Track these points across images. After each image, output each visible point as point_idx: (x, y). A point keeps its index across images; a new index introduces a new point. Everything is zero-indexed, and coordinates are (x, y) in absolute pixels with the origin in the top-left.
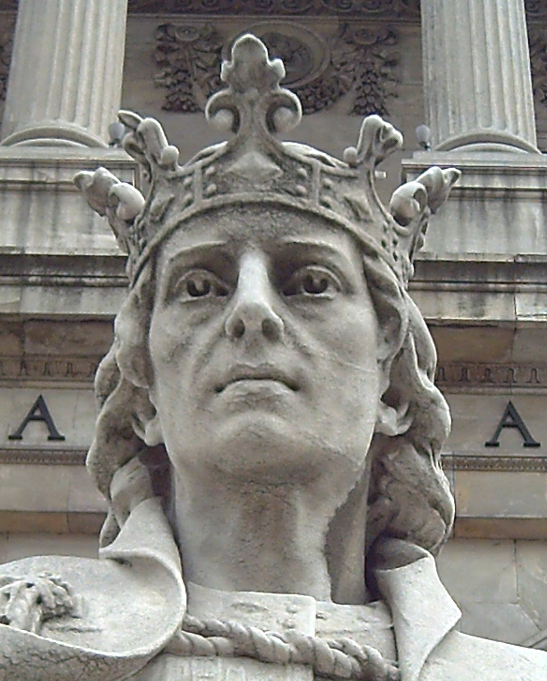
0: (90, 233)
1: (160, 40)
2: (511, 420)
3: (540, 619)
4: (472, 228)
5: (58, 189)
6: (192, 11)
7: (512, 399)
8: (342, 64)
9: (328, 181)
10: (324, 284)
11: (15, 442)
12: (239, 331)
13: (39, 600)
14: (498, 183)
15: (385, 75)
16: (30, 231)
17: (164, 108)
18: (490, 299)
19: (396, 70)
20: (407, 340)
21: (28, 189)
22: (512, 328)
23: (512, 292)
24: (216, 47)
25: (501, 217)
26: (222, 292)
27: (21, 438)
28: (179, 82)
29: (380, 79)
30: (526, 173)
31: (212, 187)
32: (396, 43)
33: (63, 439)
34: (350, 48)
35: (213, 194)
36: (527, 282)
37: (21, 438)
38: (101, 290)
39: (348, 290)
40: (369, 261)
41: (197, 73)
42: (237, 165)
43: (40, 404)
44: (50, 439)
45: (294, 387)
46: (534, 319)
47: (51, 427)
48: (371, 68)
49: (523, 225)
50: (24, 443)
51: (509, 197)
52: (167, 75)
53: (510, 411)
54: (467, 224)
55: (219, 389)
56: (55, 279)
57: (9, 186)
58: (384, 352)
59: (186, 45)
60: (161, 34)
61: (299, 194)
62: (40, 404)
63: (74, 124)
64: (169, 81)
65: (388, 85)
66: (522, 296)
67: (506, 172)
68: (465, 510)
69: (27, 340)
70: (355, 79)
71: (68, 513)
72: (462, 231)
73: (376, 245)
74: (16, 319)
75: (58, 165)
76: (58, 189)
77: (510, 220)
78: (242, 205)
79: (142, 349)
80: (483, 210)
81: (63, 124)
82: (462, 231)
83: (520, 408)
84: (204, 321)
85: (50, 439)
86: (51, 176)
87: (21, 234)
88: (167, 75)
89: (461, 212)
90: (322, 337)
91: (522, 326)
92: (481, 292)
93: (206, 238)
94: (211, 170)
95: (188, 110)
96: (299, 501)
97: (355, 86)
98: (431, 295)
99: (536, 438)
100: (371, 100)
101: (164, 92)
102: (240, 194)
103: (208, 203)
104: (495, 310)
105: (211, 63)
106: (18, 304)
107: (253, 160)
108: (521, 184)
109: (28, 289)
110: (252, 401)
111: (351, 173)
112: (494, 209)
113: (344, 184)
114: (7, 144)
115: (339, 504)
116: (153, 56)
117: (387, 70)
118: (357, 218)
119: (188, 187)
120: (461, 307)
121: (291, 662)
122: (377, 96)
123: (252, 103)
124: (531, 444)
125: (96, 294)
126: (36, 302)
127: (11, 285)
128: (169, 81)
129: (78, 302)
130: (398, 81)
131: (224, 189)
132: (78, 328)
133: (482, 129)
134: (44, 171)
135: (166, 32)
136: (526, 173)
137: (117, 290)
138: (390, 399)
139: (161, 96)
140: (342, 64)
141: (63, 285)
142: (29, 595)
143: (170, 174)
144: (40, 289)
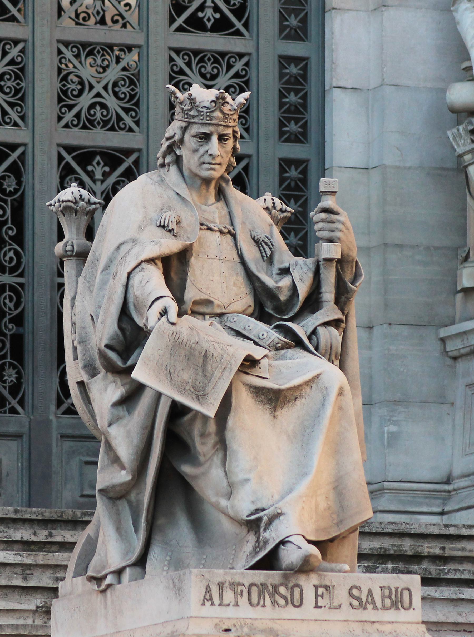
9: (231, 116)
26: (206, 139)
45: (220, 164)
78: (214, 124)
93: (206, 130)
94: (208, 114)
102: (214, 122)
107: (217, 114)
123: (220, 102)
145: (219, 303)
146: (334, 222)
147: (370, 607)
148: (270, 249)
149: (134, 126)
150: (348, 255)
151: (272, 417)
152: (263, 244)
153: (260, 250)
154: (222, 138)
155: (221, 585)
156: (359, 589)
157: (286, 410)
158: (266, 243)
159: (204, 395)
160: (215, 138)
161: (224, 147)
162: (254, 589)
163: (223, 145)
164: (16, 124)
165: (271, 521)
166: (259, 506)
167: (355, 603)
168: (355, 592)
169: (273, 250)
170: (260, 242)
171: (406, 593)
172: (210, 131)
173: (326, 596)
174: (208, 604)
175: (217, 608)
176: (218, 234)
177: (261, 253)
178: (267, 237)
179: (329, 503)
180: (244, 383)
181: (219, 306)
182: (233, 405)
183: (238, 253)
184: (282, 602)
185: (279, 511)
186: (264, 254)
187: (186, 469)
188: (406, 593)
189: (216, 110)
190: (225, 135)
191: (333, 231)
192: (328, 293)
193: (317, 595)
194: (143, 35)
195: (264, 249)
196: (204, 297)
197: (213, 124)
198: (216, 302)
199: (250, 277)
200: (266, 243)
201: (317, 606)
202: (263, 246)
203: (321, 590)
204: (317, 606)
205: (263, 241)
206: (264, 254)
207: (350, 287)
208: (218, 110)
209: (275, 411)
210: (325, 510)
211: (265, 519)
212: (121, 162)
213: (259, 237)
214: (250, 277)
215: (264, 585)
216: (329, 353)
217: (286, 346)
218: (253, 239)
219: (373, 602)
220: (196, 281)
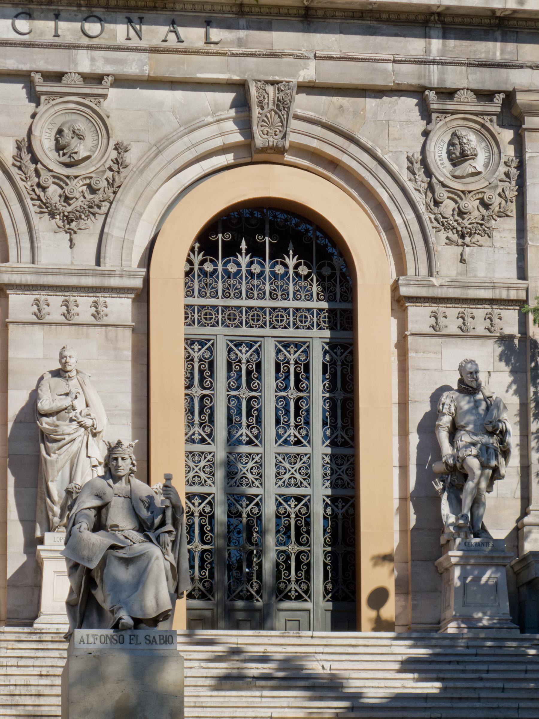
68: (152, 72)
124: (180, 41)
147: (154, 643)
149: (308, 486)
155: (88, 635)
156: (149, 636)
162: (103, 637)
164: (258, 487)
167: (148, 642)
168: (147, 637)
171: (170, 638)
173: (135, 639)
174: (82, 643)
175: (86, 645)
184: (115, 642)
187: (93, 592)
188: (170, 638)
192: (169, 520)
193: (130, 639)
194: (311, 449)
201: (130, 643)
203: (132, 637)
204: (130, 643)
212: (302, 500)
215: (107, 635)
217: (143, 542)
219: (156, 641)
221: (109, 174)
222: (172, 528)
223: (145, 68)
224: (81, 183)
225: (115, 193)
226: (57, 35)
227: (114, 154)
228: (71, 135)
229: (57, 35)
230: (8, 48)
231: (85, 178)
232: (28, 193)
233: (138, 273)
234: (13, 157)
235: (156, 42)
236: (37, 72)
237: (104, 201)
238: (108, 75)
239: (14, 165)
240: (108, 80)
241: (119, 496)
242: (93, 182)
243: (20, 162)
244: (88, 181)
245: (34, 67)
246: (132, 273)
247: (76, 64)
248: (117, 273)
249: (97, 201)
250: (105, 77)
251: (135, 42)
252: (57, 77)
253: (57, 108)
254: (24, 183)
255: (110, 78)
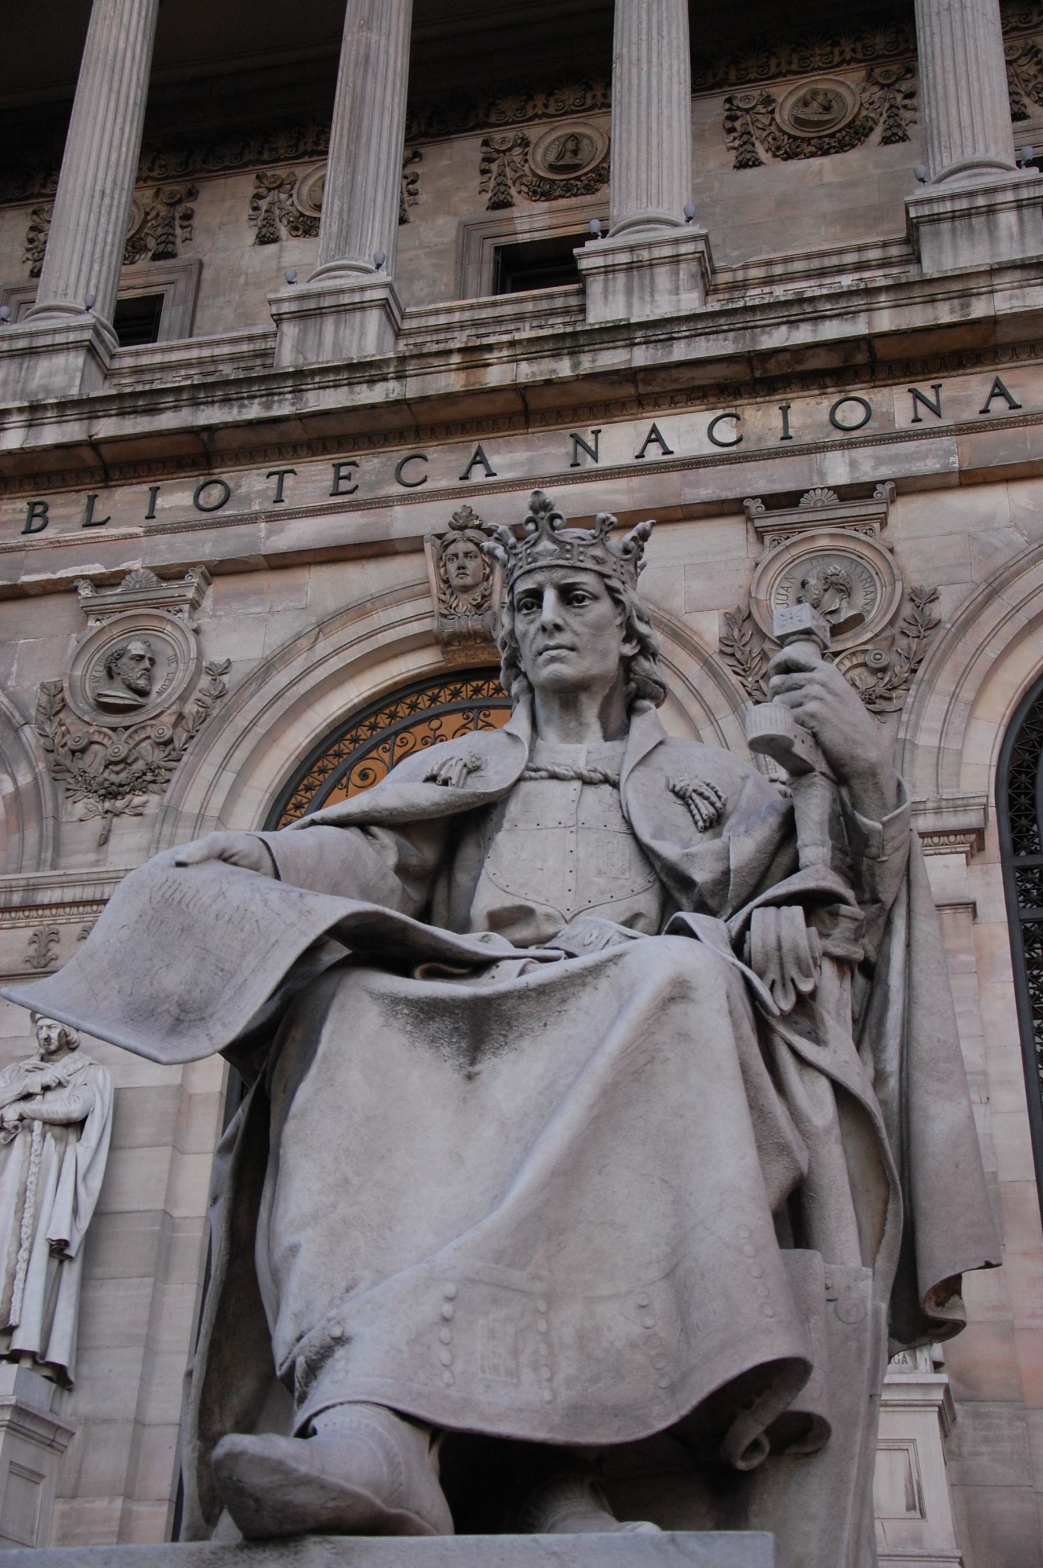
0: (678, 294)
1: (727, 110)
2: (999, 391)
3: (1029, 536)
4: (962, 242)
5: (652, 264)
6: (750, 81)
7: (999, 374)
8: (870, 104)
9: (581, 549)
10: (584, 598)
11: (640, 460)
12: (544, 629)
13: (465, 765)
14: (981, 201)
15: (905, 107)
16: (636, 300)
17: (735, 167)
18: (974, 301)
19: (914, 101)
20: (631, 612)
21: (630, 267)
22: (993, 321)
23: (992, 292)
24: (771, 108)
25: (985, 230)
27: (643, 456)
28: (745, 143)
29: (902, 111)
30: (1003, 189)
31: (530, 560)
32: (913, 77)
33: (672, 452)
34: (875, 89)
35: (530, 563)
36: (1004, 280)
37: (643, 456)
38: (686, 340)
39: (595, 598)
40: (607, 581)
41: (758, 133)
42: (540, 548)
43: (654, 430)
44: (663, 454)
45: (572, 649)
46: (1009, 311)
47: (663, 445)
48: (893, 102)
49: (1003, 232)
50: (645, 460)
51: (991, 210)
52: (735, 139)
53: (997, 384)
54: (958, 240)
55: (540, 654)
56: (653, 338)
57: (617, 267)
58: (619, 620)
59: (747, 111)
60: (728, 106)
61: (568, 559)
62: (654, 430)
63: (660, 210)
64: (737, 143)
65: (908, 115)
66: (1000, 293)
67: (988, 191)
68: (966, 464)
69: (640, 384)
70: (881, 115)
71: (681, 506)
72: (955, 246)
73: (609, 572)
74: (630, 372)
75: (650, 246)
76: (652, 264)
77: (992, 230)
79: (512, 632)
80: (970, 226)
81: (652, 212)
82: (955, 246)
83: (1005, 379)
84: (532, 621)
85: (663, 454)
86: (645, 255)
87: (629, 306)
88: (735, 139)
89: (953, 230)
90: (584, 624)
91: (1001, 318)
92: (966, 295)
94: (529, 551)
95: (754, 165)
96: (584, 698)
97: (882, 120)
98: (929, 306)
99: (1017, 401)
100: (895, 130)
101: (734, 153)
103: (527, 567)
104: (979, 309)
105: (767, 123)
106: (630, 360)
107: (546, 545)
108: (1000, 198)
109: (636, 348)
110: (553, 660)
111: (594, 541)
112: (978, 222)
113: (590, 548)
114: (613, 236)
115: (605, 694)
116: (724, 126)
117: (907, 102)
118: (598, 563)
119: (520, 559)
120: (952, 311)
121: (572, 778)
122: (899, 126)
123: (542, 519)
124: (1014, 406)
125: (683, 343)
126: (641, 357)
127: (622, 347)
128: (737, 143)
129: (671, 352)
130: (915, 109)
131: (535, 560)
132: (673, 371)
133: (969, 157)
134: (639, 252)
135: (732, 104)
136: (1003, 189)
137: (697, 339)
138: (627, 640)
139: (732, 157)
140: (870, 104)
141: (660, 341)
142: (461, 764)
143: (514, 551)
144: (644, 346)
145: (550, 910)
146: (801, 687)
148: (712, 804)
150: (852, 757)
151: (457, 1078)
152: (694, 795)
153: (691, 812)
154: (569, 596)
157: (512, 1056)
158: (701, 794)
159: (202, 1019)
160: (550, 596)
161: (580, 615)
163: (578, 610)
165: (313, 1369)
166: (304, 1326)
169: (718, 805)
170: (688, 794)
172: (536, 583)
176: (577, 784)
177: (693, 816)
178: (708, 785)
179: (649, 1322)
180: (371, 993)
181: (549, 917)
182: (322, 1049)
183: (624, 817)
185: (337, 1332)
186: (698, 817)
189: (539, 537)
190: (572, 587)
191: (800, 705)
195: (696, 806)
196: (508, 902)
197: (541, 568)
198: (540, 910)
199: (646, 854)
200: (701, 794)
202: (693, 801)
205: (694, 791)
206: (698, 817)
207: (865, 825)
208: (544, 537)
209: (473, 1062)
210: (633, 1346)
211: (301, 1361)
213: (682, 784)
214: (646, 854)
216: (775, 960)
218: (673, 791)
220: (498, 874)
221: (903, 642)
222: (834, 883)
223: (952, 459)
224: (848, 664)
225: (914, 671)
226: (786, 437)
227: (908, 610)
228: (821, 586)
229: (786, 437)
230: (701, 470)
231: (854, 654)
232: (749, 694)
233: (972, 801)
234: (720, 641)
235: (970, 414)
236: (754, 498)
237: (895, 688)
238: (883, 482)
239: (722, 652)
240: (884, 491)
241: (554, 776)
242: (869, 659)
243: (732, 646)
244: (860, 659)
245: (749, 491)
246: (960, 802)
247: (822, 474)
248: (930, 805)
249: (880, 690)
250: (879, 487)
251: (930, 421)
252: (790, 500)
253: (794, 552)
254: (740, 678)
255: (889, 486)
